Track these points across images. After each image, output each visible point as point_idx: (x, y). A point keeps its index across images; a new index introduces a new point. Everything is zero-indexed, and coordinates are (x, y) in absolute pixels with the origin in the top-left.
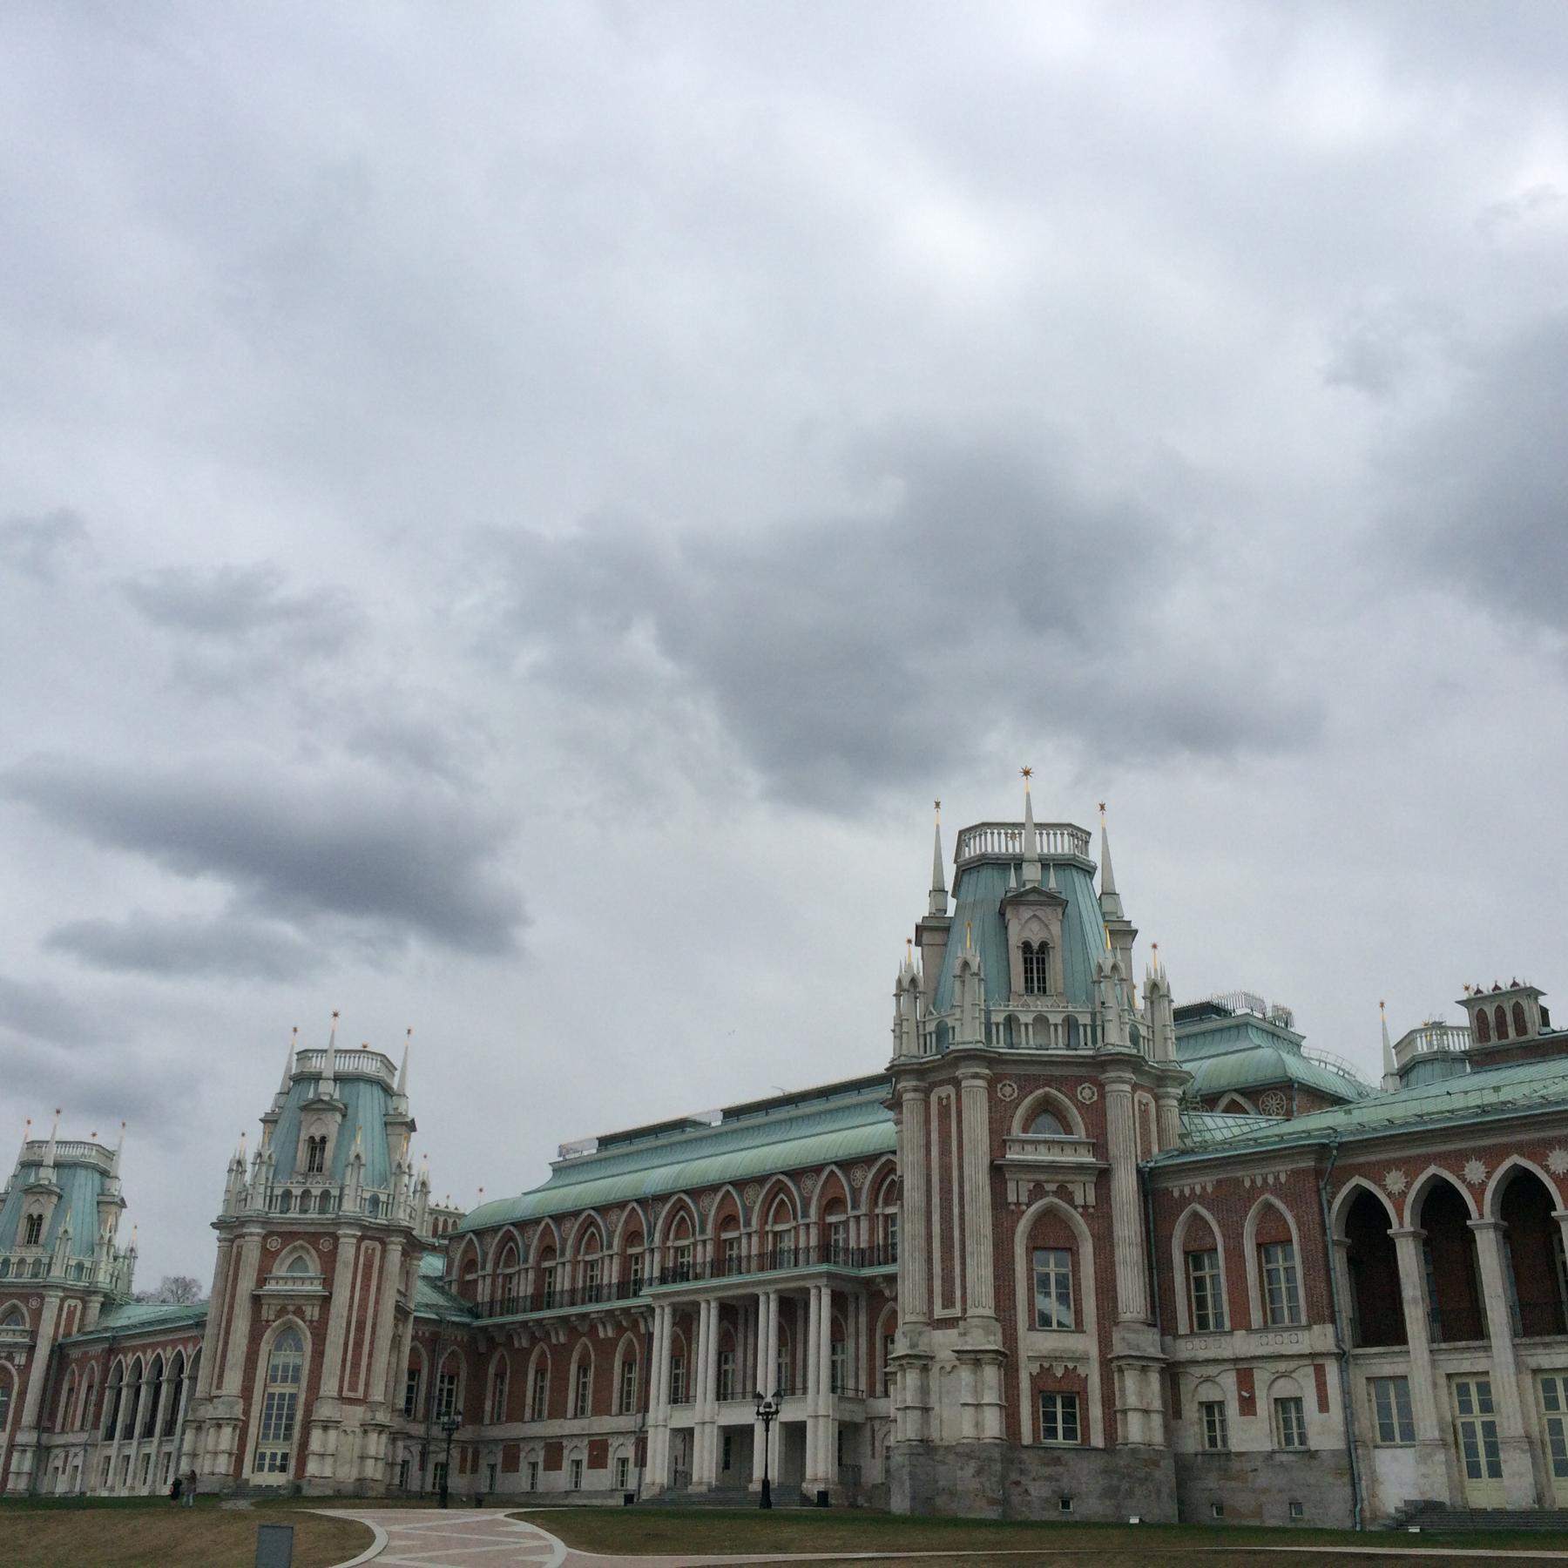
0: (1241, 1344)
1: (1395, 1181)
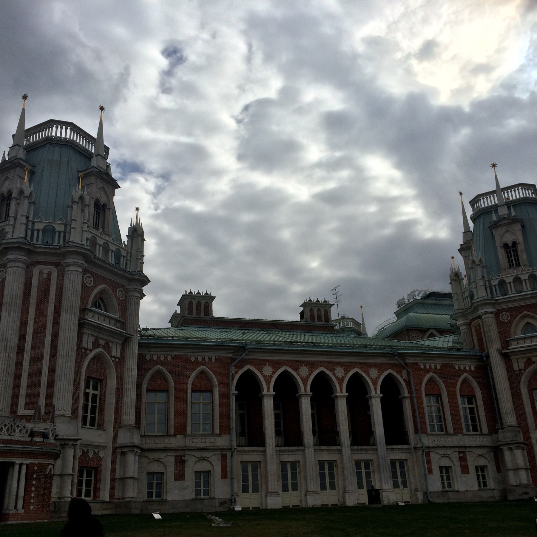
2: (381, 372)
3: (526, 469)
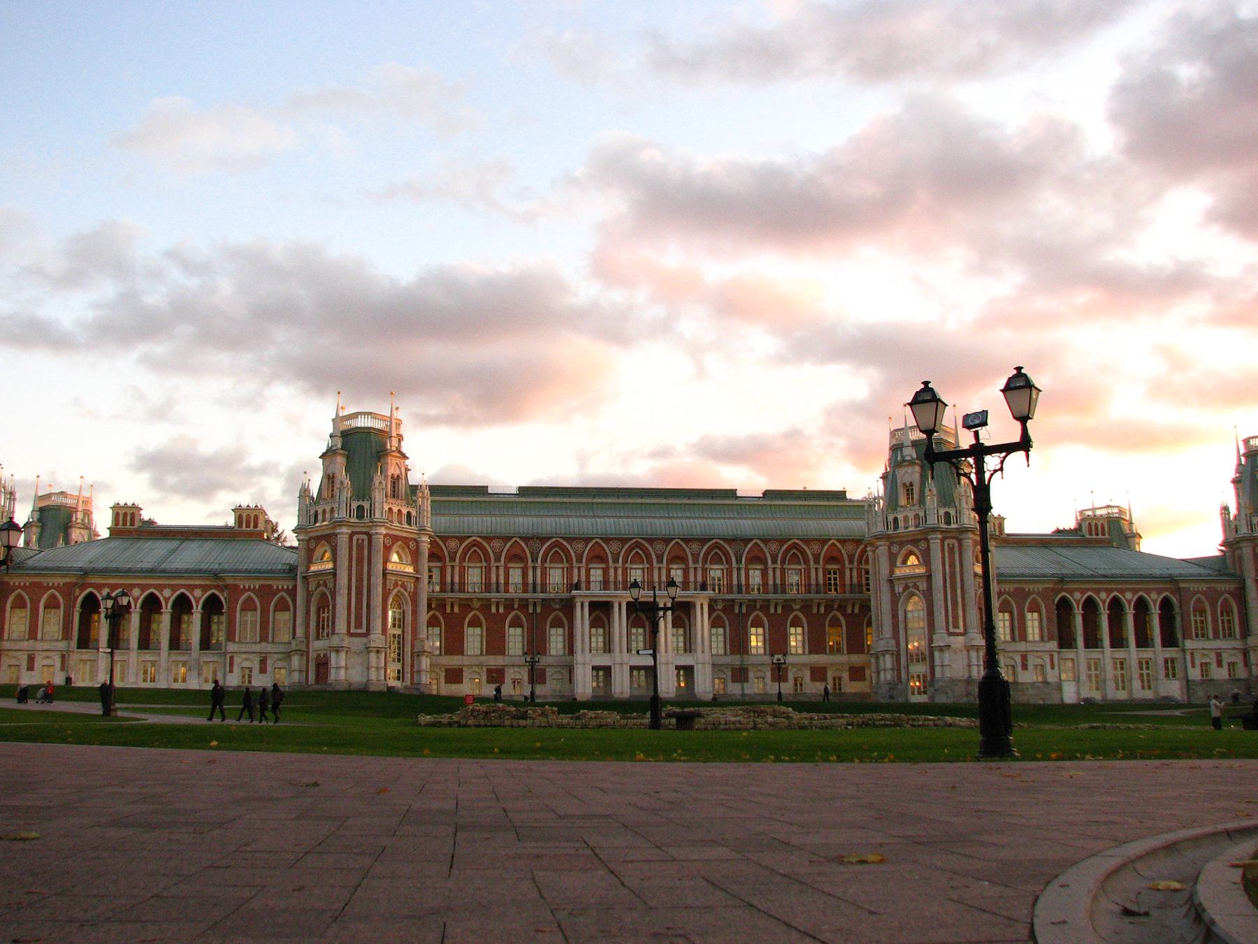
0: (1021, 646)
1: (1077, 595)
2: (204, 592)
3: (301, 671)
